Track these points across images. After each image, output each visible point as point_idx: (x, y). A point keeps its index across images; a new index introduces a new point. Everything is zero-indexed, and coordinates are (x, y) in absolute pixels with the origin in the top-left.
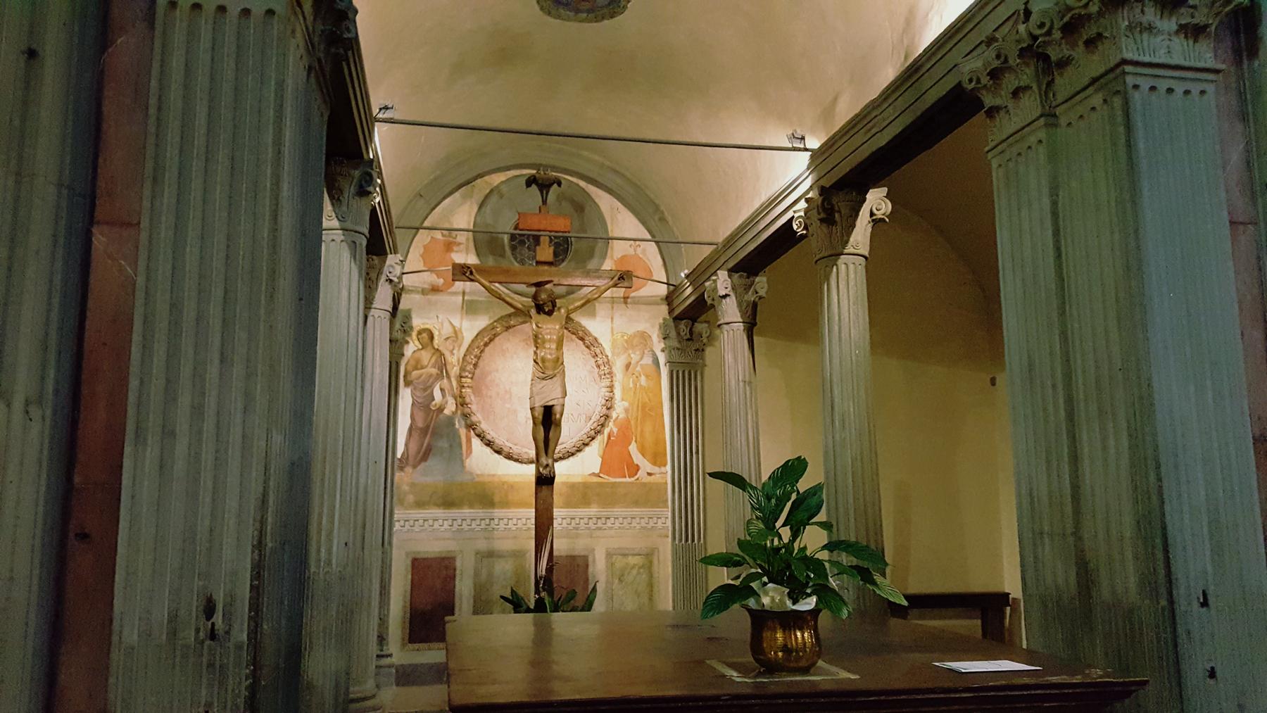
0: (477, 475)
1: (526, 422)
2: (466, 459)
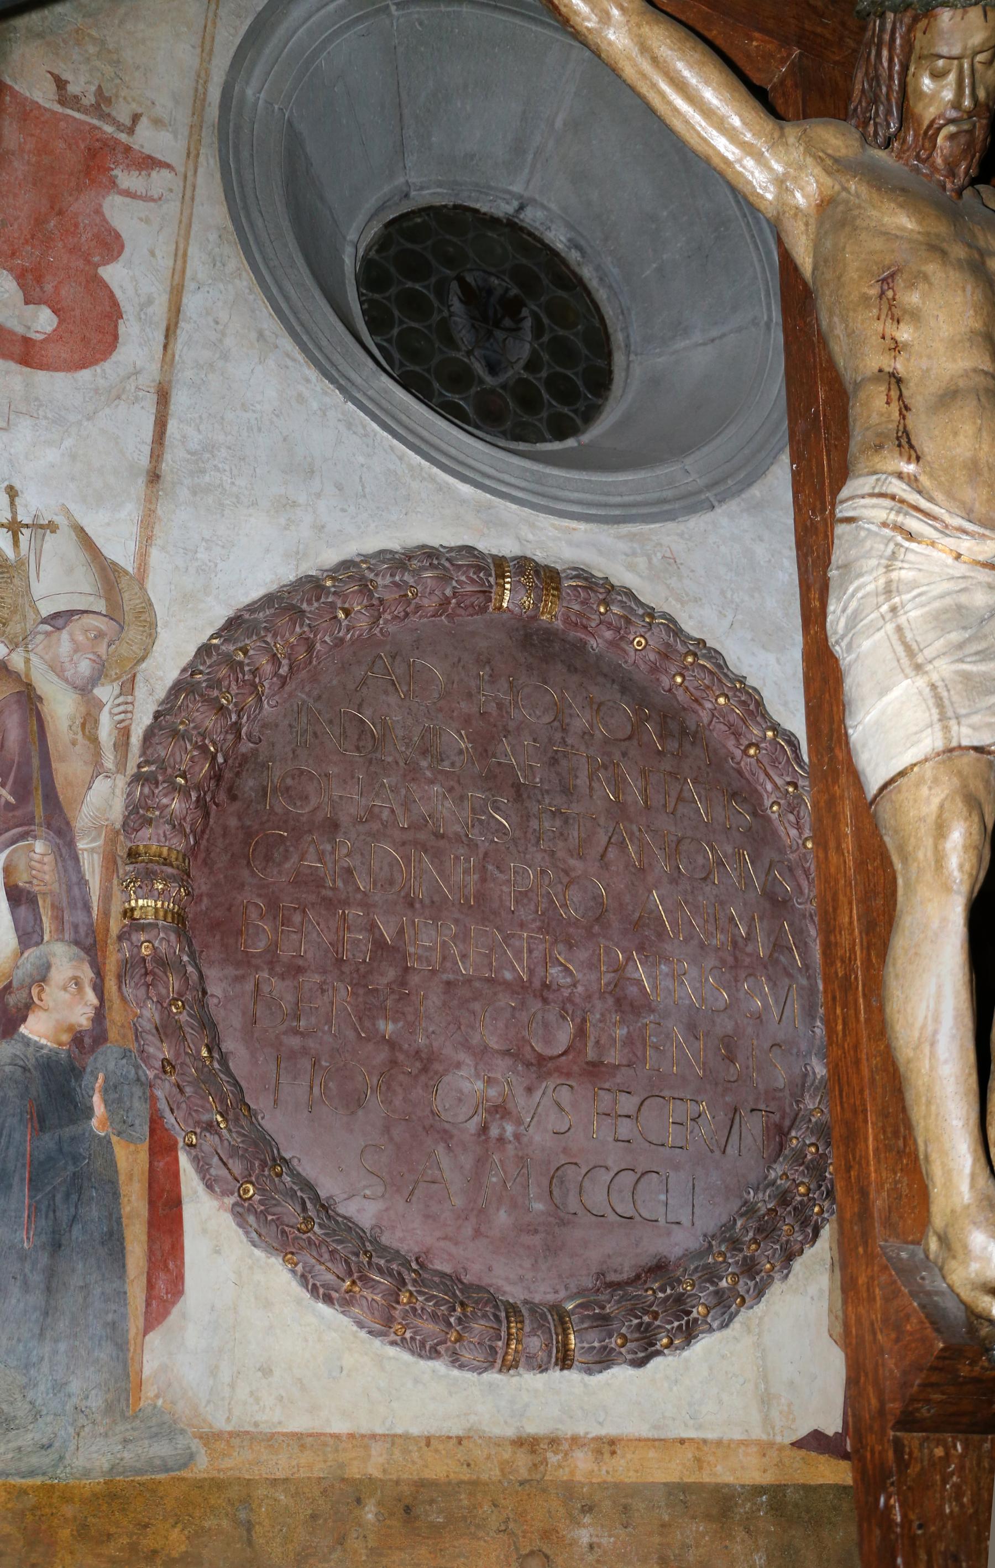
0: (211, 1438)
1: (484, 1129)
2: (148, 1328)
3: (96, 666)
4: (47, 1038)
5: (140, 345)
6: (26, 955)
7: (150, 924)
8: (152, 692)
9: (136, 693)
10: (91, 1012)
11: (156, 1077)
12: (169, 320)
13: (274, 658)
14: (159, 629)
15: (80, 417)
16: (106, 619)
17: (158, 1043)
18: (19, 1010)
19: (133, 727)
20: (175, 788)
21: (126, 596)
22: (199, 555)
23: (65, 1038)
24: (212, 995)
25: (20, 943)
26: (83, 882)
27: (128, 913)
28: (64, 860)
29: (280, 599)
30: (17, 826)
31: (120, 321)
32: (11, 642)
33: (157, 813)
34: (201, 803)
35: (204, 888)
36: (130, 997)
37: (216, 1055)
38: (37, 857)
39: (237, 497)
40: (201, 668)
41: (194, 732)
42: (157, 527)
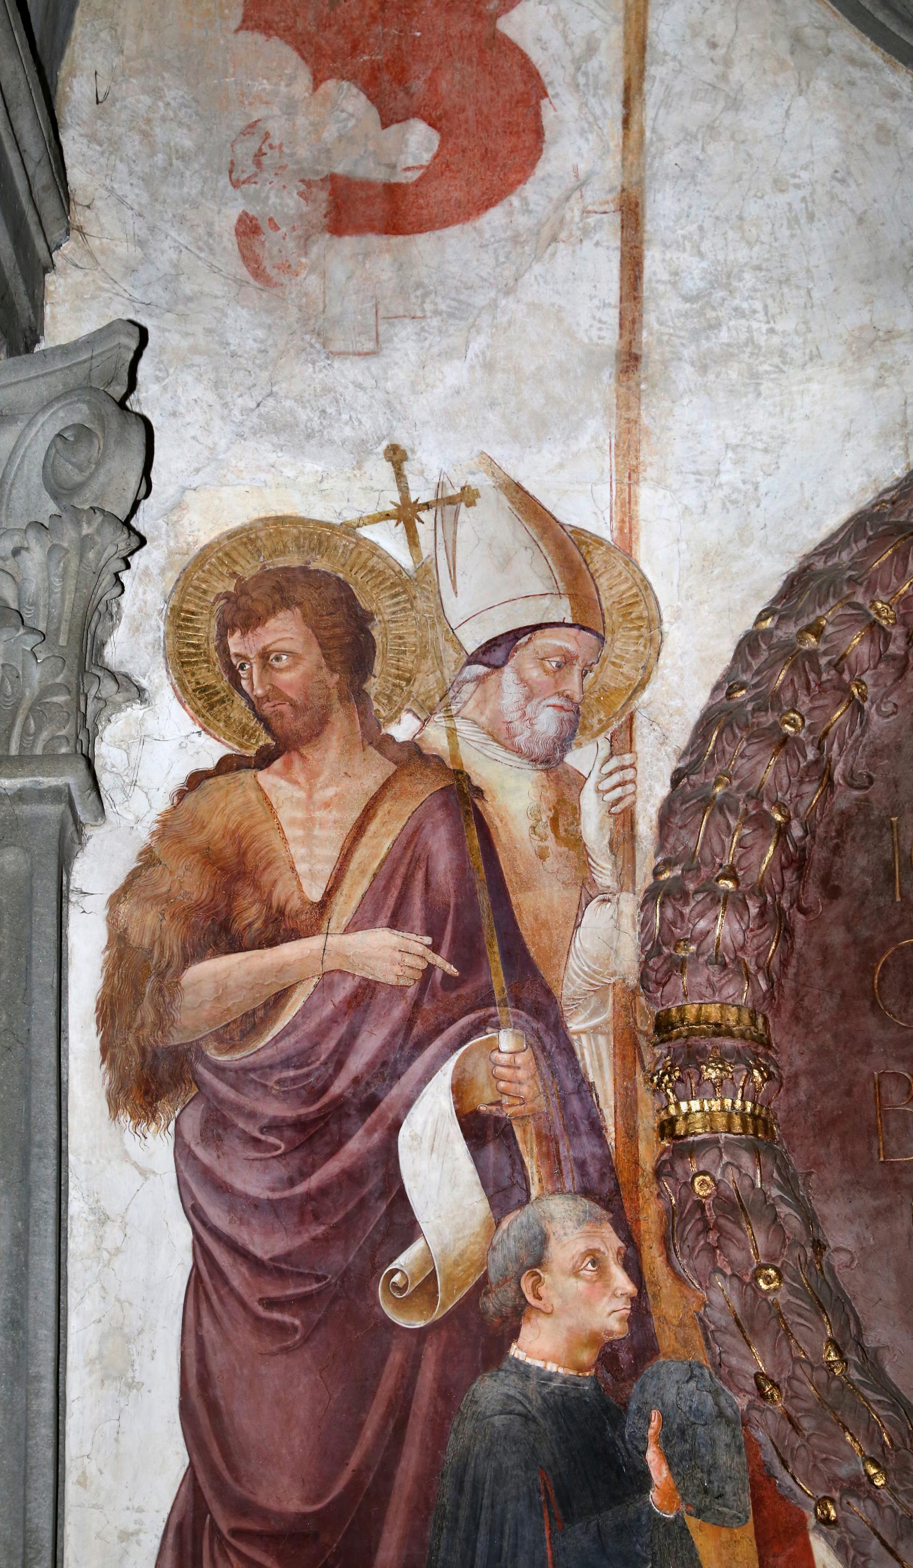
3: (565, 715)
4: (556, 1360)
5: (582, 133)
6: (504, 1225)
7: (704, 1142)
8: (664, 739)
9: (638, 746)
10: (623, 1307)
11: (751, 1406)
12: (628, 70)
13: (874, 630)
14: (665, 627)
15: (492, 294)
16: (573, 631)
17: (742, 1348)
18: (504, 1319)
19: (639, 807)
20: (717, 899)
21: (603, 582)
22: (724, 478)
23: (587, 1356)
24: (838, 1250)
25: (492, 1207)
26: (584, 1088)
27: (666, 1128)
28: (549, 1056)
29: (880, 515)
30: (466, 1013)
31: (544, 102)
32: (422, 708)
33: (693, 948)
34: (771, 916)
35: (800, 1063)
36: (688, 1274)
37: (852, 1357)
38: (504, 1058)
39: (782, 354)
40: (744, 678)
41: (742, 795)
42: (644, 448)
